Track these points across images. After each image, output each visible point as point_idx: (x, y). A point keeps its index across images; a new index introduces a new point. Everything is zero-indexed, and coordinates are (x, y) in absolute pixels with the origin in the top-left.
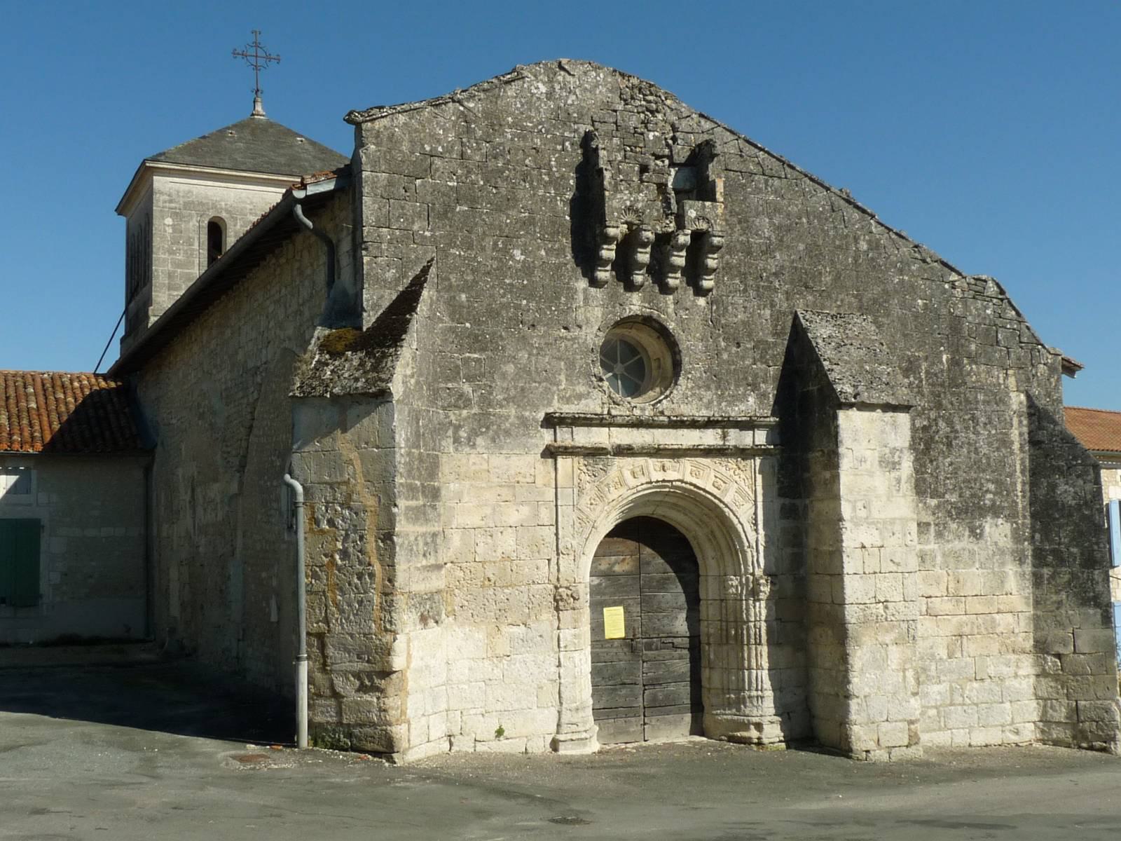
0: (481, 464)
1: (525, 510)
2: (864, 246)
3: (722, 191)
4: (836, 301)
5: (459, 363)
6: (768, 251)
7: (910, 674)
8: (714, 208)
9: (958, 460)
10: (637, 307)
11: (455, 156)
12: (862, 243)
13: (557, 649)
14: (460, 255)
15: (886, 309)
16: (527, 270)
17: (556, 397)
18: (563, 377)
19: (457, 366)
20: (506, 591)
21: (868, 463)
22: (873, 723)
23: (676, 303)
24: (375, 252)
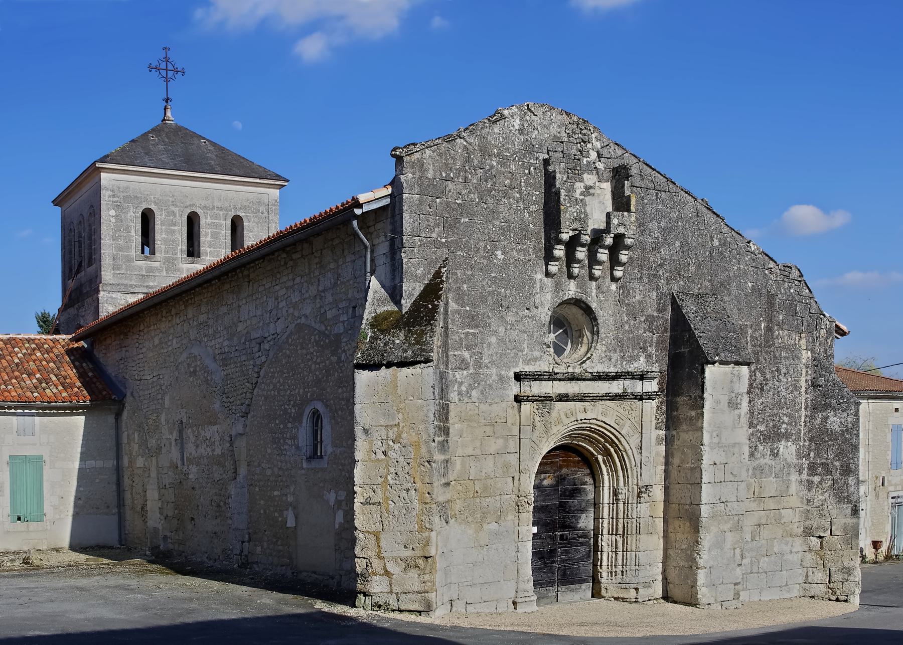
0: (474, 410)
1: (500, 442)
2: (716, 243)
3: (635, 203)
4: (698, 284)
5: (463, 336)
6: (656, 248)
7: (738, 551)
8: (630, 216)
9: (767, 400)
10: (573, 292)
11: (460, 180)
12: (715, 240)
13: (516, 539)
14: (463, 256)
15: (728, 290)
16: (505, 265)
17: (521, 360)
18: (525, 346)
19: (461, 339)
20: (487, 500)
21: (722, 404)
22: (714, 585)
23: (598, 288)
24: (411, 255)
